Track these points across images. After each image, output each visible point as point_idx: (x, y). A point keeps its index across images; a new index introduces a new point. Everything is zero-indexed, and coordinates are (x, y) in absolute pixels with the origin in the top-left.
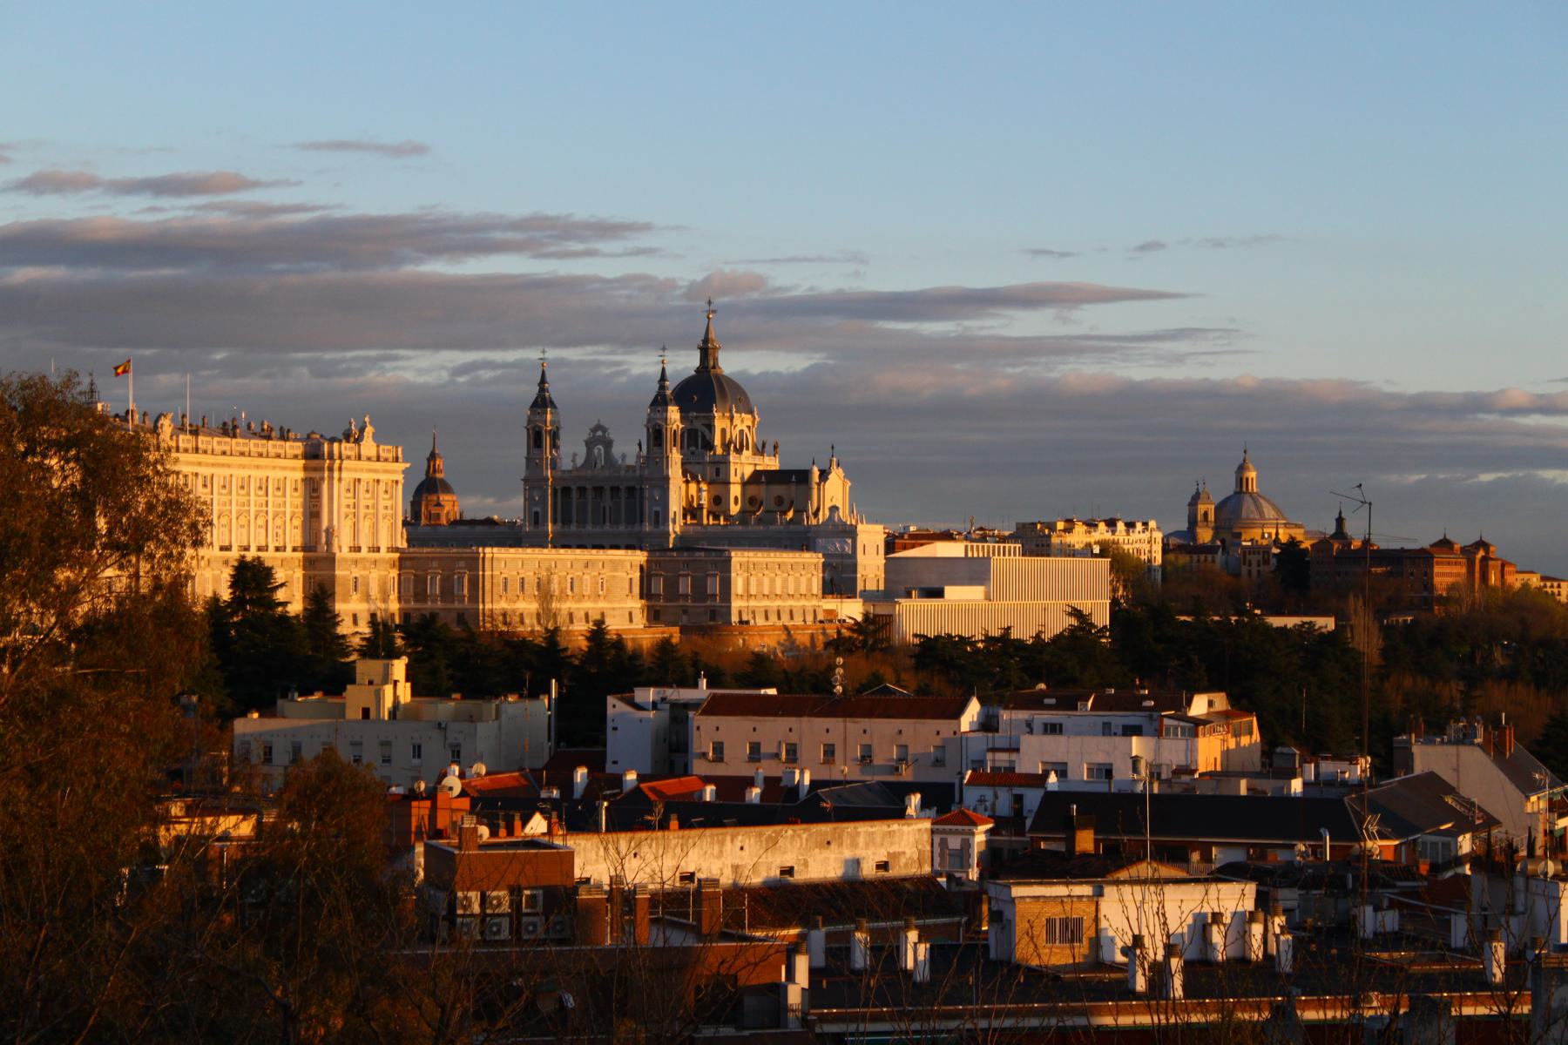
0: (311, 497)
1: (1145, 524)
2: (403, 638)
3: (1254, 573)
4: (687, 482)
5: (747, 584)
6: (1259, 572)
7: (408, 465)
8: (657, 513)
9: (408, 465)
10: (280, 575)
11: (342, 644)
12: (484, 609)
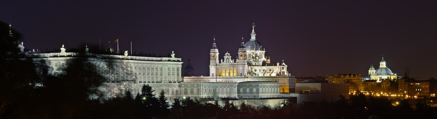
0: (160, 70)
1: (358, 75)
2: (182, 103)
3: (385, 87)
4: (248, 66)
5: (263, 90)
6: (386, 86)
7: (183, 63)
8: (241, 73)
9: (183, 63)
10: (153, 89)
11: (168, 104)
12: (201, 96)
